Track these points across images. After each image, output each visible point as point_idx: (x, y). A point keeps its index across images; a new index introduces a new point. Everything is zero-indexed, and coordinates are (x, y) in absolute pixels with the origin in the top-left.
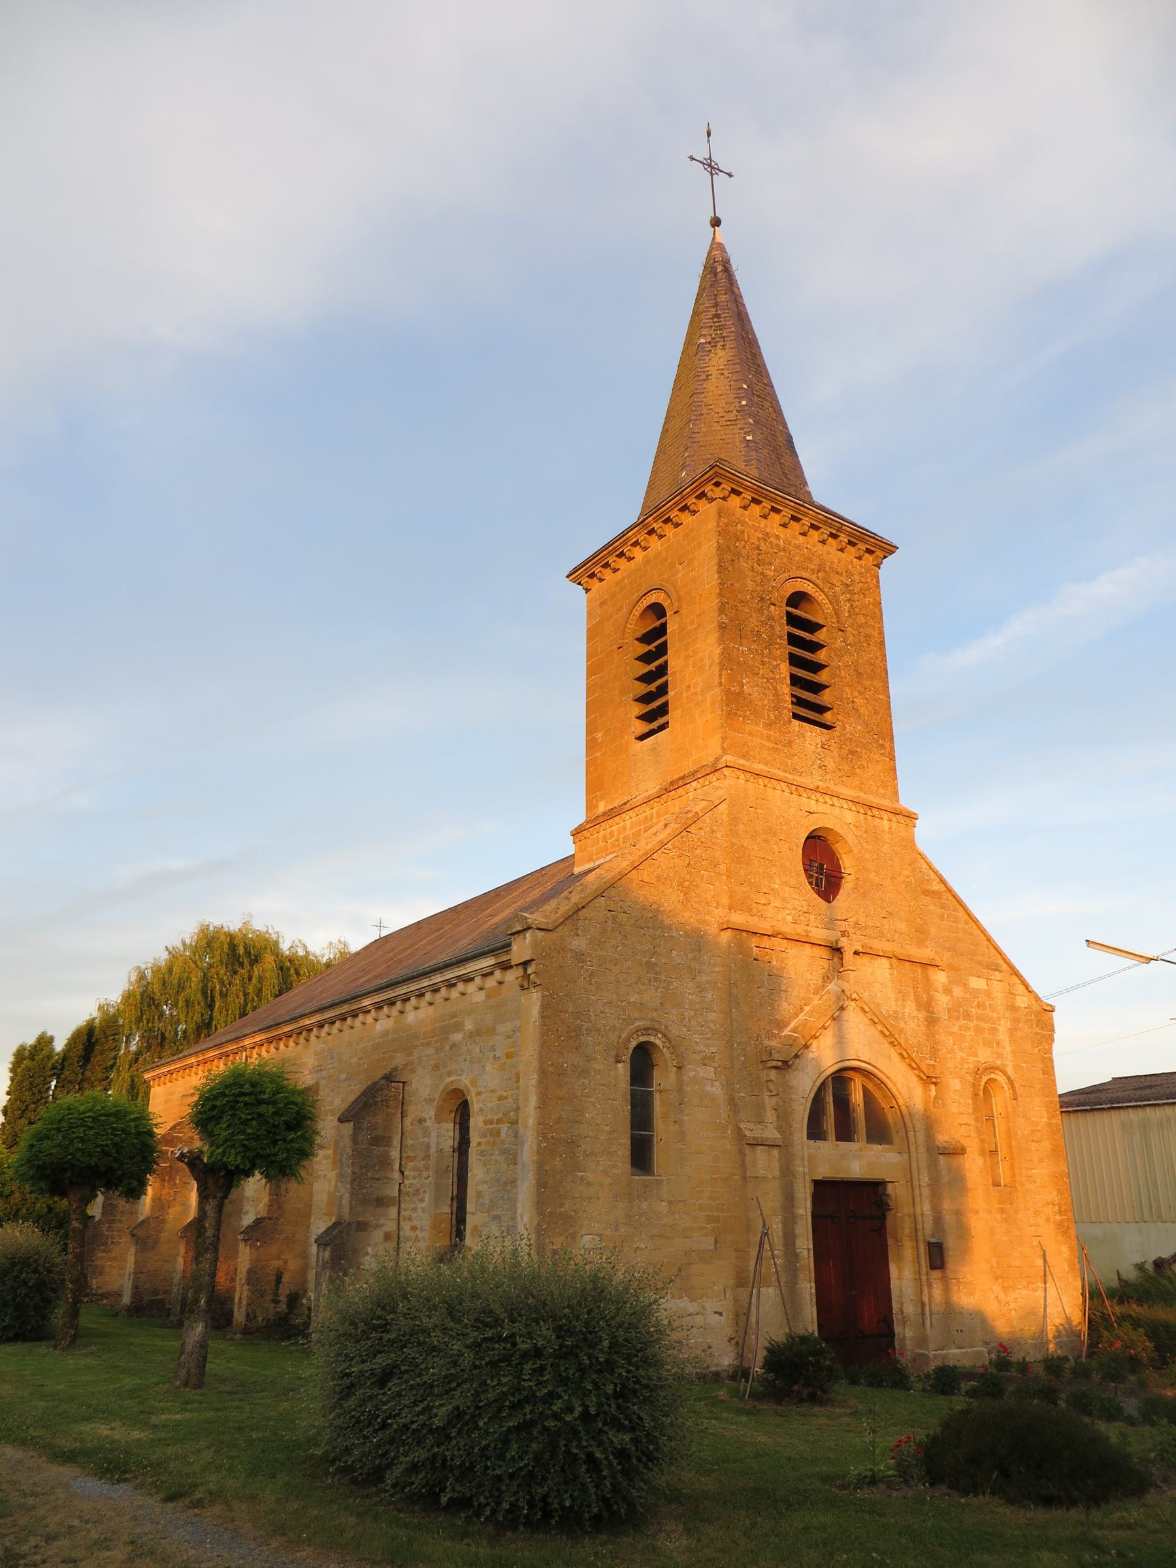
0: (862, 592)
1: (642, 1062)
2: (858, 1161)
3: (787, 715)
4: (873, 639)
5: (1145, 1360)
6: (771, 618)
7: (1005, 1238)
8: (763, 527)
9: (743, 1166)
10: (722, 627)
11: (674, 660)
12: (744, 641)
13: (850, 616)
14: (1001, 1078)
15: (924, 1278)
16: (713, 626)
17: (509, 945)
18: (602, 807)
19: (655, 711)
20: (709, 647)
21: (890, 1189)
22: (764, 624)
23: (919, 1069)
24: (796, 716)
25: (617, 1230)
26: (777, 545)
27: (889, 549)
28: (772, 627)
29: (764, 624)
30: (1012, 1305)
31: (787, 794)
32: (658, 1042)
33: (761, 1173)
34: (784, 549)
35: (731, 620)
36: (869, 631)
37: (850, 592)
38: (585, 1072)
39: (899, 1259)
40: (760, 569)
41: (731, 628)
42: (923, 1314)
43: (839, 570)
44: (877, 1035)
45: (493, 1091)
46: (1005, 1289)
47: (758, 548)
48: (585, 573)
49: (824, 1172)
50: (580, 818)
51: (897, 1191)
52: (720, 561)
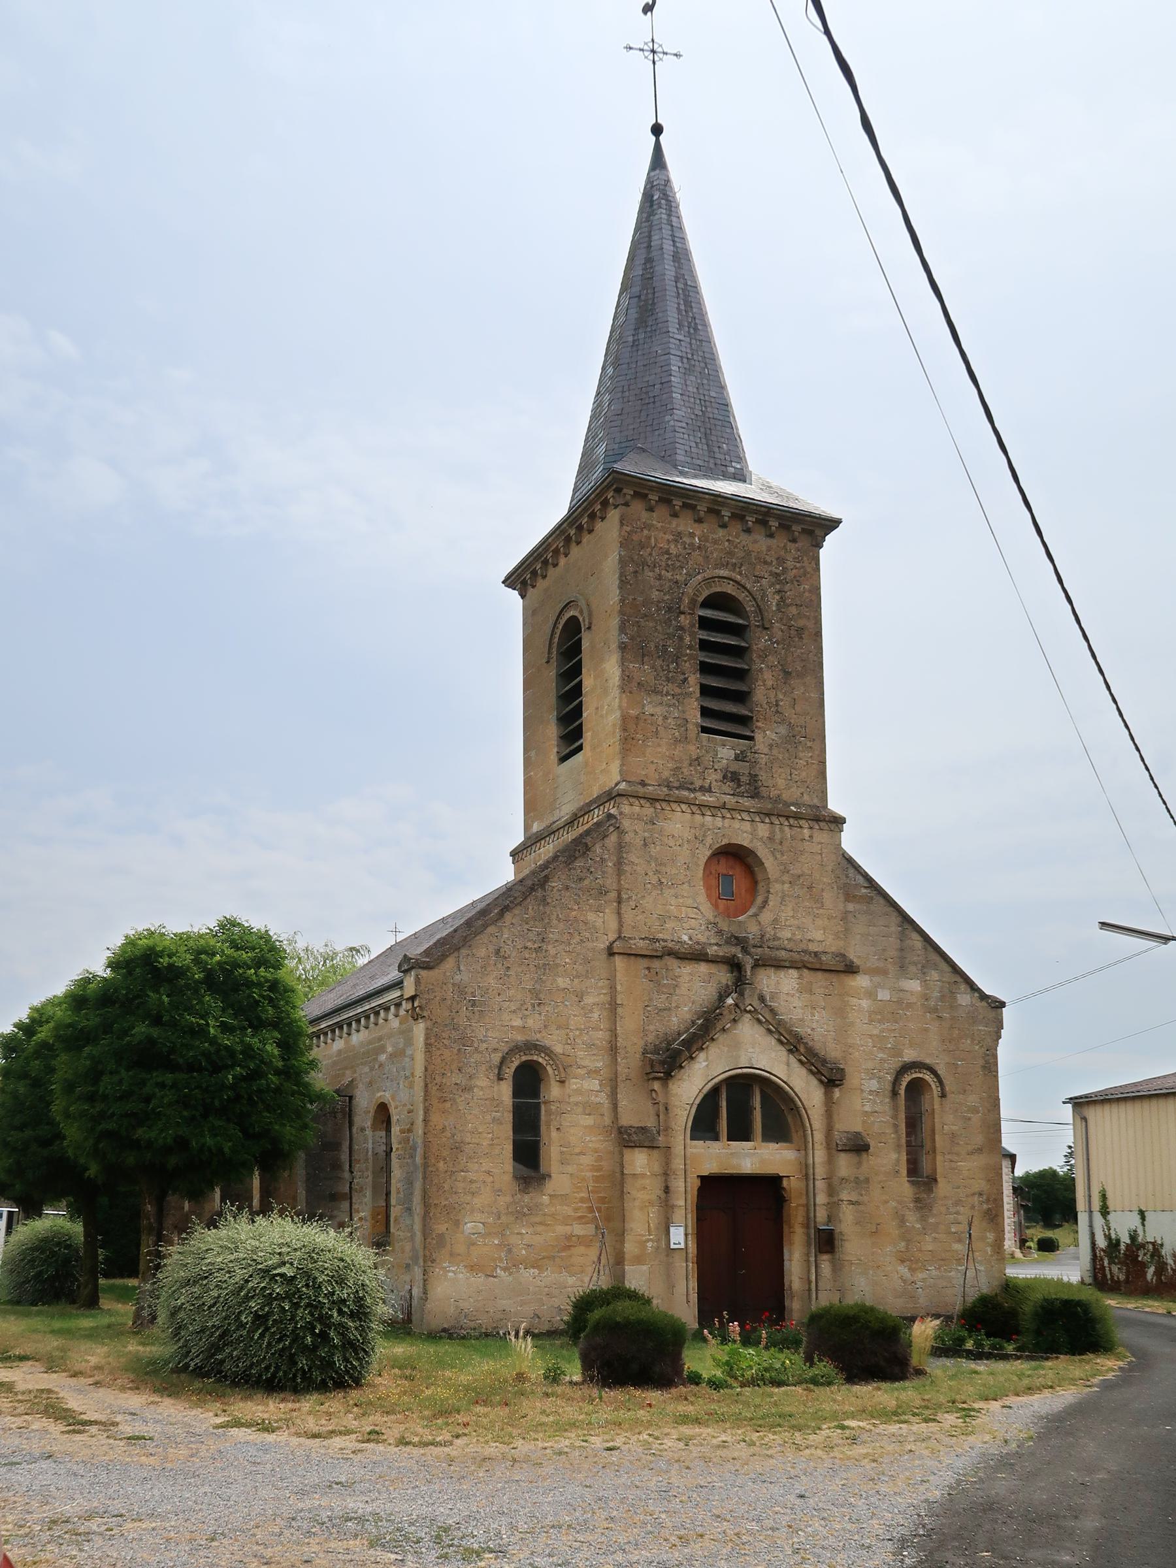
0: (797, 580)
1: (528, 1081)
2: (753, 1157)
3: (693, 730)
4: (808, 633)
5: (796, 1308)
6: (682, 628)
7: (918, 1226)
8: (664, 530)
9: (622, 1166)
10: (623, 647)
11: (588, 681)
12: (646, 659)
13: (779, 610)
14: (928, 1077)
15: (812, 1259)
16: (614, 646)
17: (401, 982)
18: (536, 827)
19: (571, 735)
20: (612, 668)
21: (785, 1183)
22: (670, 636)
23: (819, 1072)
24: (705, 730)
25: (499, 1218)
26: (692, 545)
27: (823, 526)
28: (681, 638)
29: (670, 636)
30: (919, 1284)
31: (688, 816)
32: (540, 1060)
33: (639, 1171)
34: (699, 548)
35: (632, 638)
36: (801, 623)
37: (780, 582)
38: (468, 1089)
39: (791, 1244)
40: (669, 575)
41: (634, 648)
42: (810, 1290)
43: (768, 559)
44: (774, 1042)
45: (405, 1105)
46: (912, 1270)
47: (667, 552)
48: (520, 579)
49: (710, 1167)
50: (519, 838)
51: (792, 1185)
52: (621, 575)
